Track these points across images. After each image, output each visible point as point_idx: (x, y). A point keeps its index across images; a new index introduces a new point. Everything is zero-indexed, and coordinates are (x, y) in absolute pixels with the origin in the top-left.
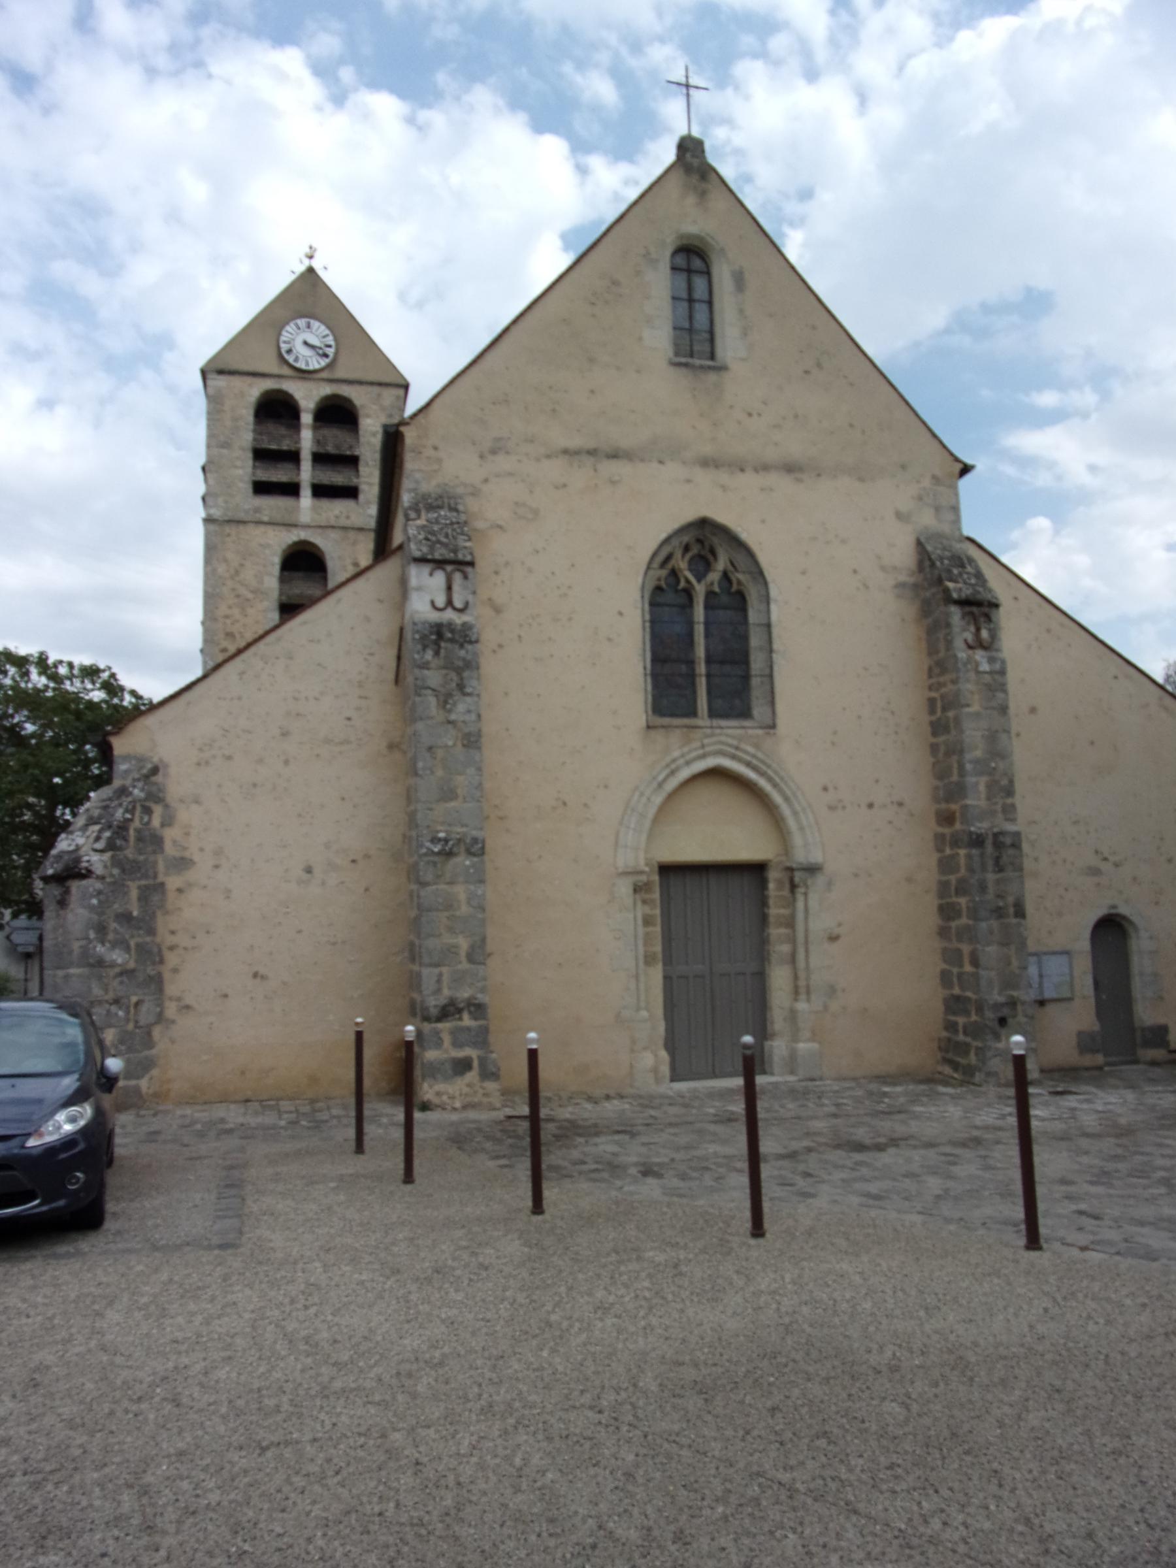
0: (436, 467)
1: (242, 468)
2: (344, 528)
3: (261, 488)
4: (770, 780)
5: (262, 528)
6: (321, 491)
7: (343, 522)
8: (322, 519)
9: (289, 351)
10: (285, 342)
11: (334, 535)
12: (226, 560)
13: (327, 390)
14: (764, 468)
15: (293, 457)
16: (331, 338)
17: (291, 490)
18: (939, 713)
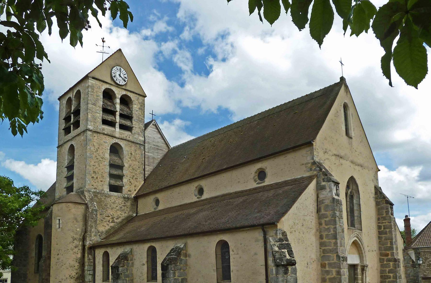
2: (129, 141)
3: (105, 122)
4: (362, 243)
5: (105, 136)
6: (122, 127)
7: (128, 138)
8: (122, 136)
9: (115, 76)
11: (125, 142)
12: (94, 145)
13: (124, 93)
14: (358, 165)
15: (113, 113)
16: (126, 75)
17: (112, 124)
18: (382, 229)
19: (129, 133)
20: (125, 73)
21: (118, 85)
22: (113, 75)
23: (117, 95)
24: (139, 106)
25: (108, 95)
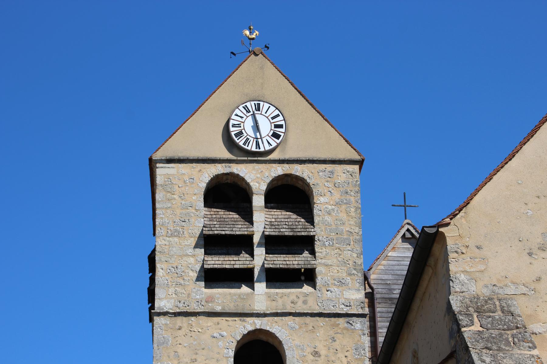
0: (482, 267)
1: (193, 256)
3: (212, 277)
6: (277, 277)
7: (300, 308)
10: (234, 126)
13: (279, 170)
17: (244, 277)
19: (307, 289)
20: (277, 112)
21: (256, 157)
22: (233, 131)
23: (254, 186)
24: (337, 196)
25: (227, 194)
